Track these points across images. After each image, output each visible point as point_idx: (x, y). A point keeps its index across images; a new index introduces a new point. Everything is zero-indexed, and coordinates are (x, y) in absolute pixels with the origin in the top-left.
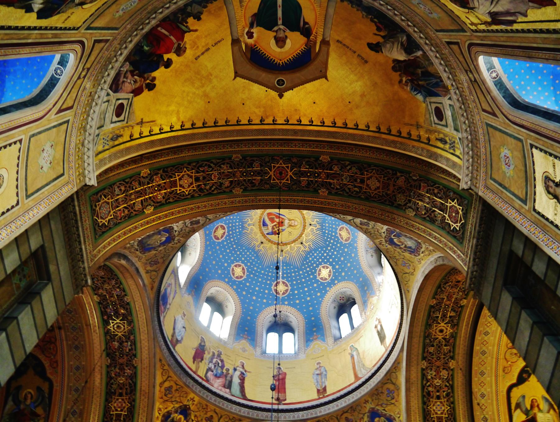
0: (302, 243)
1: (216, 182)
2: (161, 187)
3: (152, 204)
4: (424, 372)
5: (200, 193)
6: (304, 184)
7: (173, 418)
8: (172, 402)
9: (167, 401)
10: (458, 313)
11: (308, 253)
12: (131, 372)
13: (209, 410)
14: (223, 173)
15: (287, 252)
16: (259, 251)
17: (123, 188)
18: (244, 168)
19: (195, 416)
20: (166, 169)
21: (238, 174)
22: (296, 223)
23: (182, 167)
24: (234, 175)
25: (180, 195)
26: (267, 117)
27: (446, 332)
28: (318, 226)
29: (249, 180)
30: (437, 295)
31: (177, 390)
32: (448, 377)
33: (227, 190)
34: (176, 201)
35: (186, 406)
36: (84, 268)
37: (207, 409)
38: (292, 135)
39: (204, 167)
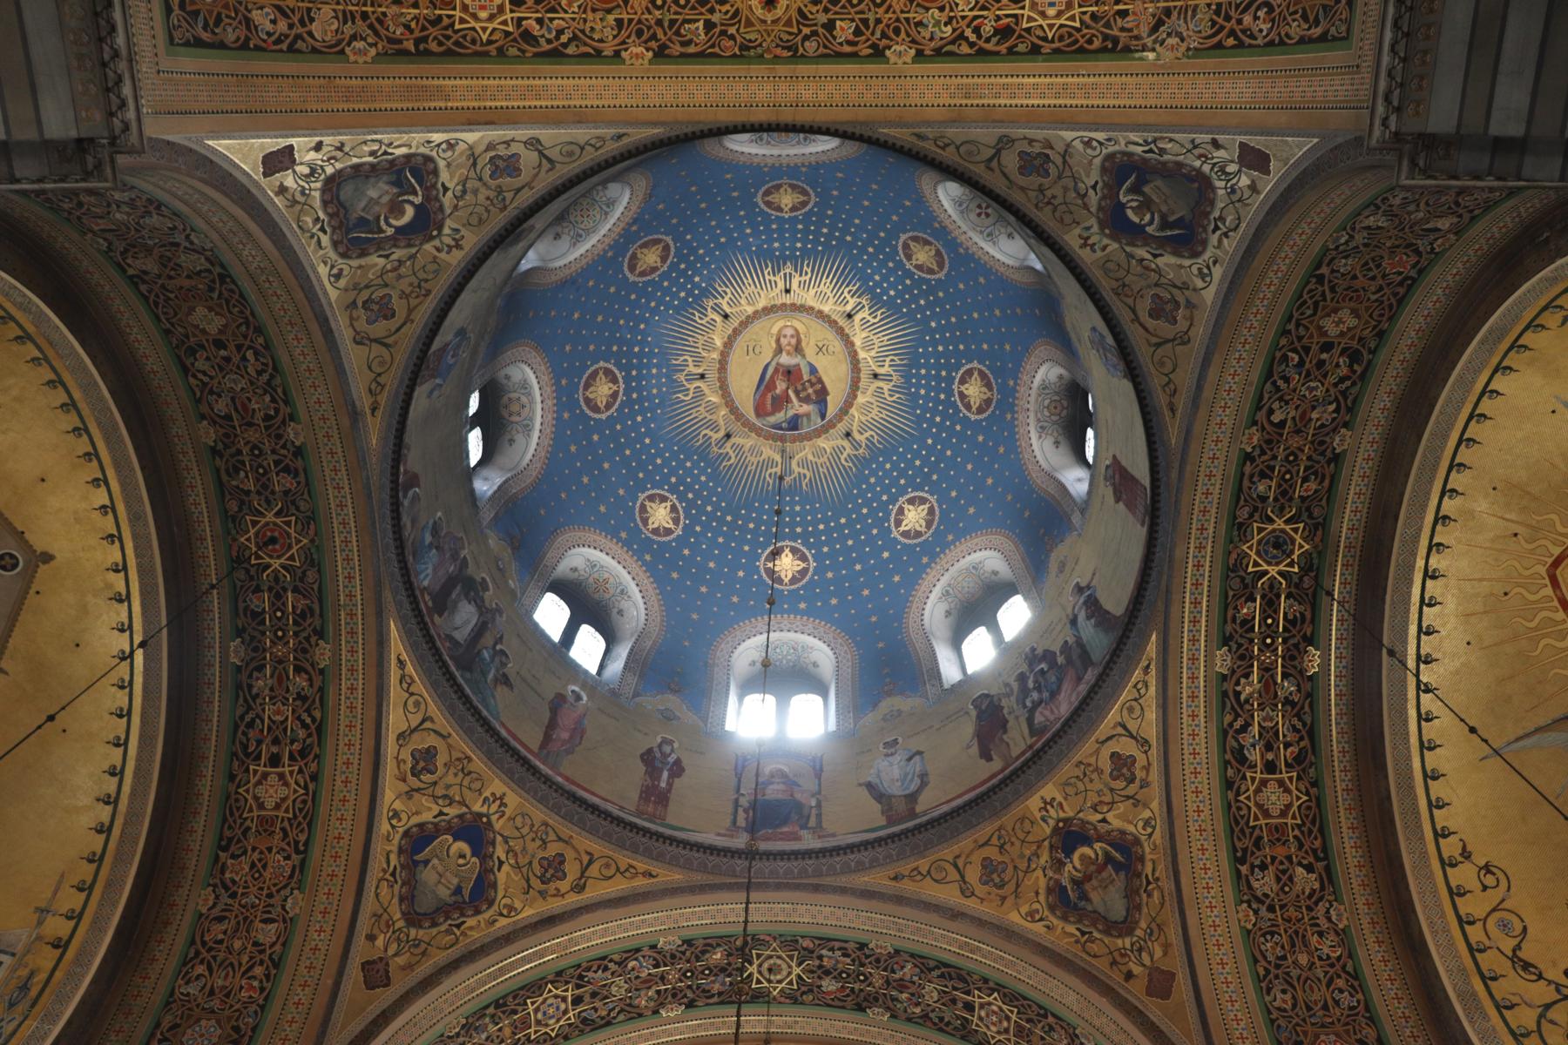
0: (850, 316)
1: (293, 711)
2: (260, 860)
4: (928, 52)
5: (311, 757)
6: (287, 482)
7: (1074, 881)
9: (1018, 886)
11: (876, 302)
12: (909, 966)
13: (1092, 760)
14: (272, 689)
15: (880, 361)
16: (870, 444)
17: (200, 969)
18: (263, 633)
19: (1095, 808)
20: (223, 843)
21: (280, 650)
22: (789, 332)
23: (233, 797)
24: (280, 662)
26: (109, 586)
28: (789, 269)
29: (296, 623)
30: (599, 53)
31: (1001, 847)
33: (317, 682)
34: (310, 825)
35: (1056, 830)
37: (1089, 765)
38: (146, 525)
39: (248, 740)
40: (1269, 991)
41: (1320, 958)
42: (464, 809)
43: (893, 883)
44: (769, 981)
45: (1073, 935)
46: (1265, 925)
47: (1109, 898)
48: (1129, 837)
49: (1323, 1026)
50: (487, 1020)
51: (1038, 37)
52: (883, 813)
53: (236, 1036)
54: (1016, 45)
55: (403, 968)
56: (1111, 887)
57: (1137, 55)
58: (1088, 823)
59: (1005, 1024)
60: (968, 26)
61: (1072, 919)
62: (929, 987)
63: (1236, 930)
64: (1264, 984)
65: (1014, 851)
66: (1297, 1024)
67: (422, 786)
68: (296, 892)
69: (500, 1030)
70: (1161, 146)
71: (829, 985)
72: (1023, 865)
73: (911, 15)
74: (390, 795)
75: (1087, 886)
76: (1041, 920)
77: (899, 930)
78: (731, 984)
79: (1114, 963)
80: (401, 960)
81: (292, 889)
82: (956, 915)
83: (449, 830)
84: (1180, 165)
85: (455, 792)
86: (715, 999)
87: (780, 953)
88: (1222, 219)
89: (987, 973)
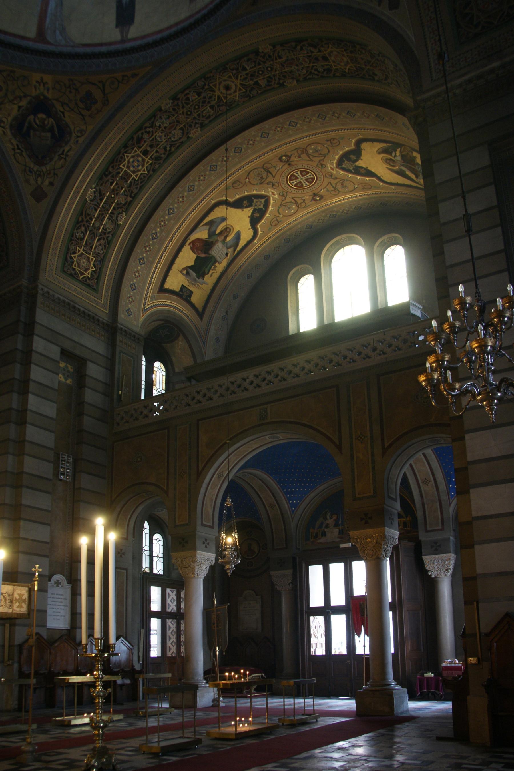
10: (268, 88)
27: (230, 94)
32: (177, 141)
51: (128, 150)
54: (132, 141)
57: (97, 181)
60: (152, 131)
70: (63, 160)
73: (174, 118)
84: (51, 159)
88: (21, 155)
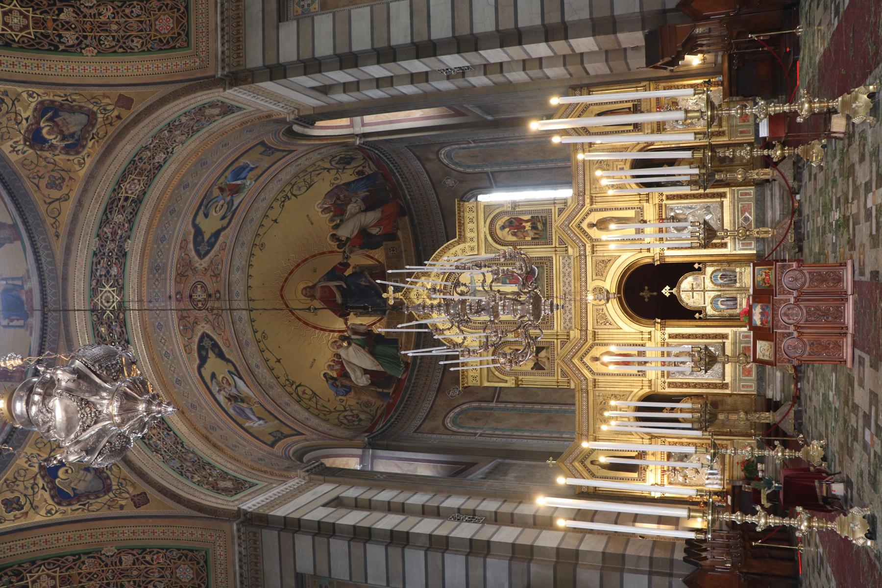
3: (103, 557)
8: (55, 164)
9: (63, 170)
12: (105, 229)
25: (54, 564)
31: (40, 177)
34: (62, 557)
35: (31, 146)
36: (239, 545)
40: (131, 48)
41: (114, 18)
42: (38, 476)
43: (61, 238)
44: (113, 302)
45: (94, 143)
46: (95, 43)
47: (74, 123)
48: (38, 106)
49: (151, 26)
50: (151, 442)
52: (11, 242)
53: (184, 557)
55: (135, 488)
56: (67, 121)
58: (28, 128)
59: (136, 181)
61: (85, 143)
62: (116, 219)
63: (98, 59)
64: (128, 51)
65: (42, 171)
66: (150, 38)
67: (28, 502)
68: (103, 552)
69: (154, 435)
71: (114, 271)
72: (51, 167)
74: (39, 518)
75: (66, 133)
76: (84, 159)
77: (87, 235)
78: (116, 322)
79: (111, 124)
80: (131, 490)
81: (101, 555)
82: (80, 204)
83: (53, 482)
85: (29, 484)
86: (124, 329)
87: (99, 297)
89: (110, 189)
